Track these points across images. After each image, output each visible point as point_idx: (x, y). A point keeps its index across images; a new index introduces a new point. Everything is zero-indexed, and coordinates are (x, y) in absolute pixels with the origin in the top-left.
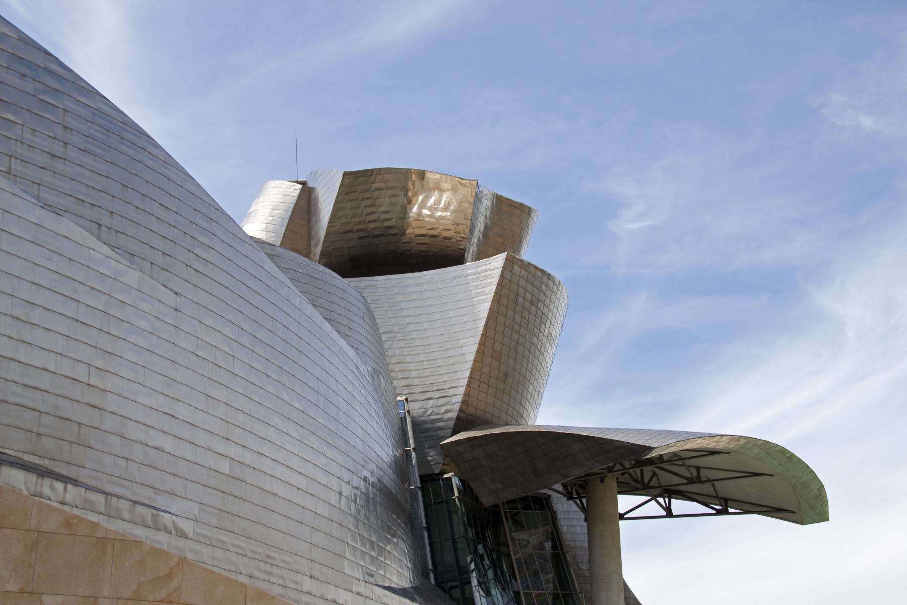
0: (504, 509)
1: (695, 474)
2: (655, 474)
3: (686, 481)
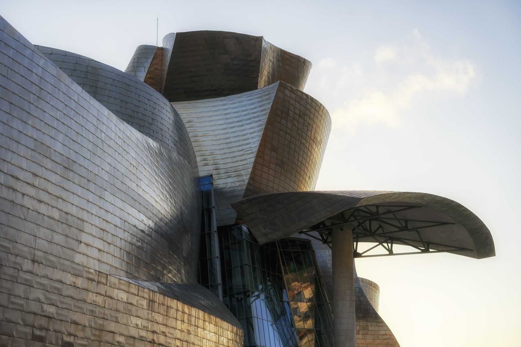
0: (280, 248)
1: (404, 225)
2: (380, 227)
3: (398, 230)
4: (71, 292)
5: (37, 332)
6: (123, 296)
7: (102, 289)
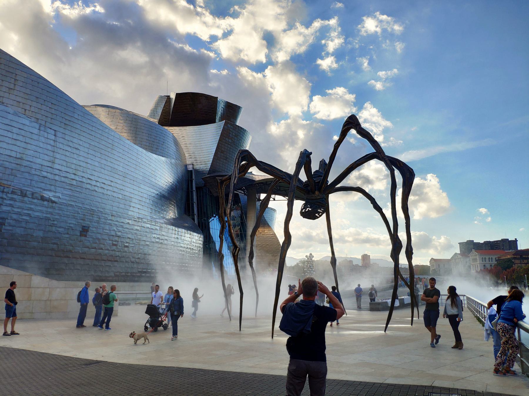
4: (127, 226)
5: (114, 243)
6: (149, 226)
7: (140, 224)
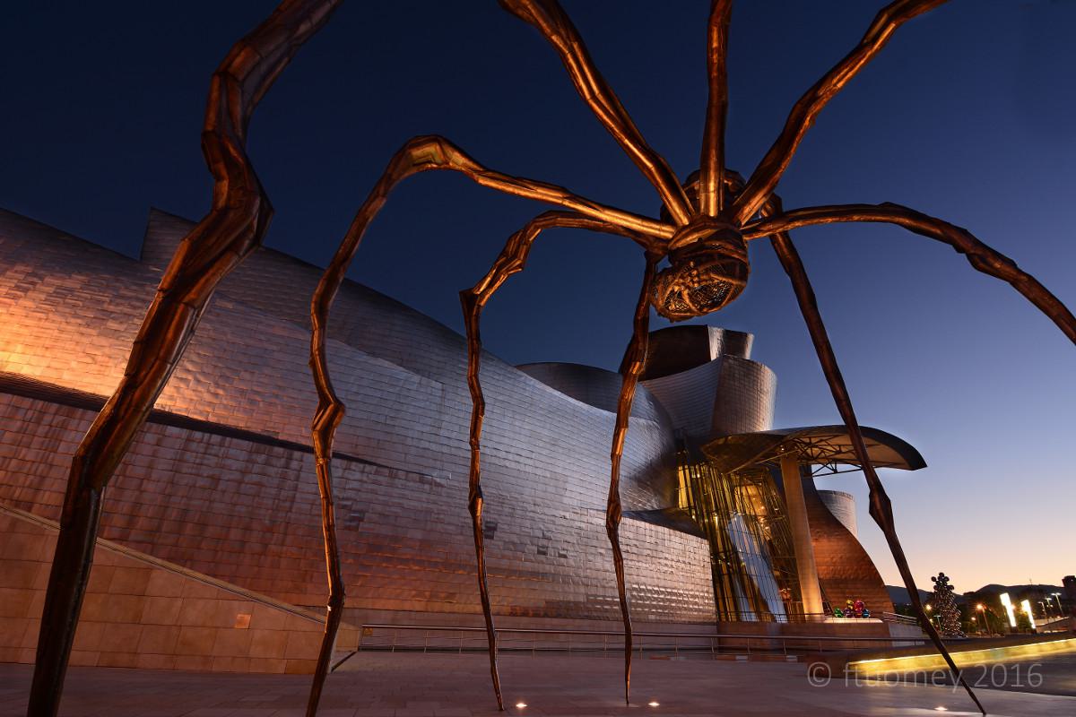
4: (563, 522)
7: (584, 519)
